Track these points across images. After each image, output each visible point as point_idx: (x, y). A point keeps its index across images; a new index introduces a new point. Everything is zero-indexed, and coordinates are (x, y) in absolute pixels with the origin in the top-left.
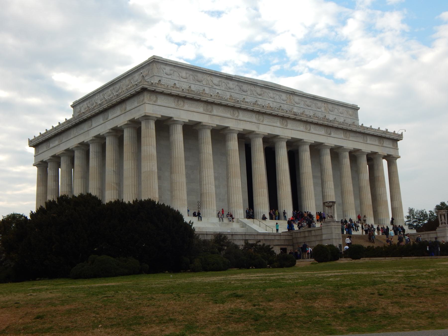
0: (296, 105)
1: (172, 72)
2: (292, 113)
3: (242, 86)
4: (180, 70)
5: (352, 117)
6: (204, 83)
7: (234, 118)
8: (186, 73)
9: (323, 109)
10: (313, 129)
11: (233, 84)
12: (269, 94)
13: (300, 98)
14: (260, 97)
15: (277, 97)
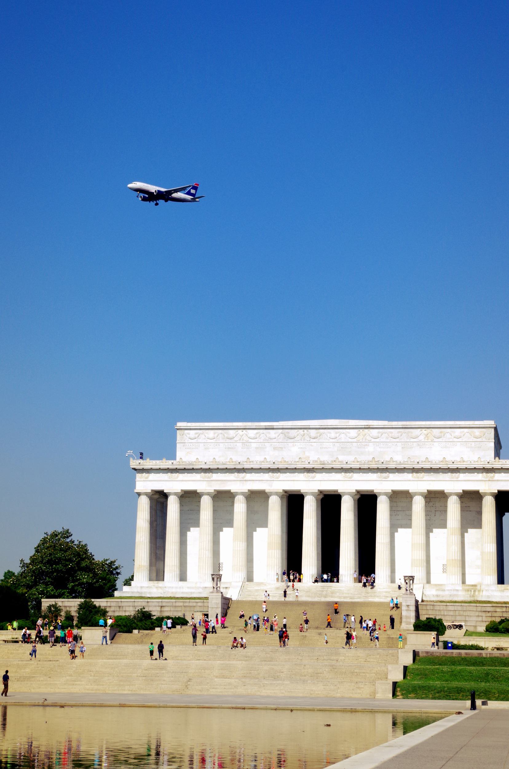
0: (373, 440)
1: (197, 435)
2: (319, 463)
3: (288, 433)
4: (207, 431)
5: (479, 440)
6: (235, 439)
7: (239, 479)
8: (215, 433)
9: (422, 438)
10: (356, 476)
11: (275, 433)
12: (329, 435)
13: (381, 430)
14: (314, 440)
15: (343, 436)
